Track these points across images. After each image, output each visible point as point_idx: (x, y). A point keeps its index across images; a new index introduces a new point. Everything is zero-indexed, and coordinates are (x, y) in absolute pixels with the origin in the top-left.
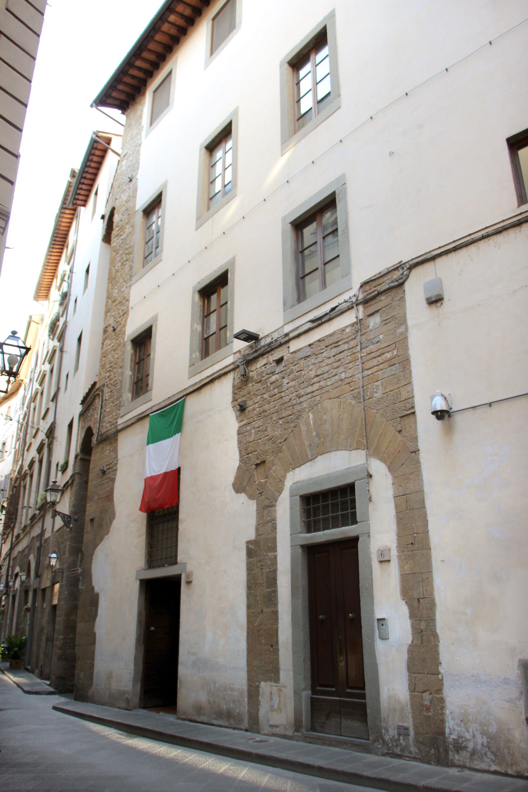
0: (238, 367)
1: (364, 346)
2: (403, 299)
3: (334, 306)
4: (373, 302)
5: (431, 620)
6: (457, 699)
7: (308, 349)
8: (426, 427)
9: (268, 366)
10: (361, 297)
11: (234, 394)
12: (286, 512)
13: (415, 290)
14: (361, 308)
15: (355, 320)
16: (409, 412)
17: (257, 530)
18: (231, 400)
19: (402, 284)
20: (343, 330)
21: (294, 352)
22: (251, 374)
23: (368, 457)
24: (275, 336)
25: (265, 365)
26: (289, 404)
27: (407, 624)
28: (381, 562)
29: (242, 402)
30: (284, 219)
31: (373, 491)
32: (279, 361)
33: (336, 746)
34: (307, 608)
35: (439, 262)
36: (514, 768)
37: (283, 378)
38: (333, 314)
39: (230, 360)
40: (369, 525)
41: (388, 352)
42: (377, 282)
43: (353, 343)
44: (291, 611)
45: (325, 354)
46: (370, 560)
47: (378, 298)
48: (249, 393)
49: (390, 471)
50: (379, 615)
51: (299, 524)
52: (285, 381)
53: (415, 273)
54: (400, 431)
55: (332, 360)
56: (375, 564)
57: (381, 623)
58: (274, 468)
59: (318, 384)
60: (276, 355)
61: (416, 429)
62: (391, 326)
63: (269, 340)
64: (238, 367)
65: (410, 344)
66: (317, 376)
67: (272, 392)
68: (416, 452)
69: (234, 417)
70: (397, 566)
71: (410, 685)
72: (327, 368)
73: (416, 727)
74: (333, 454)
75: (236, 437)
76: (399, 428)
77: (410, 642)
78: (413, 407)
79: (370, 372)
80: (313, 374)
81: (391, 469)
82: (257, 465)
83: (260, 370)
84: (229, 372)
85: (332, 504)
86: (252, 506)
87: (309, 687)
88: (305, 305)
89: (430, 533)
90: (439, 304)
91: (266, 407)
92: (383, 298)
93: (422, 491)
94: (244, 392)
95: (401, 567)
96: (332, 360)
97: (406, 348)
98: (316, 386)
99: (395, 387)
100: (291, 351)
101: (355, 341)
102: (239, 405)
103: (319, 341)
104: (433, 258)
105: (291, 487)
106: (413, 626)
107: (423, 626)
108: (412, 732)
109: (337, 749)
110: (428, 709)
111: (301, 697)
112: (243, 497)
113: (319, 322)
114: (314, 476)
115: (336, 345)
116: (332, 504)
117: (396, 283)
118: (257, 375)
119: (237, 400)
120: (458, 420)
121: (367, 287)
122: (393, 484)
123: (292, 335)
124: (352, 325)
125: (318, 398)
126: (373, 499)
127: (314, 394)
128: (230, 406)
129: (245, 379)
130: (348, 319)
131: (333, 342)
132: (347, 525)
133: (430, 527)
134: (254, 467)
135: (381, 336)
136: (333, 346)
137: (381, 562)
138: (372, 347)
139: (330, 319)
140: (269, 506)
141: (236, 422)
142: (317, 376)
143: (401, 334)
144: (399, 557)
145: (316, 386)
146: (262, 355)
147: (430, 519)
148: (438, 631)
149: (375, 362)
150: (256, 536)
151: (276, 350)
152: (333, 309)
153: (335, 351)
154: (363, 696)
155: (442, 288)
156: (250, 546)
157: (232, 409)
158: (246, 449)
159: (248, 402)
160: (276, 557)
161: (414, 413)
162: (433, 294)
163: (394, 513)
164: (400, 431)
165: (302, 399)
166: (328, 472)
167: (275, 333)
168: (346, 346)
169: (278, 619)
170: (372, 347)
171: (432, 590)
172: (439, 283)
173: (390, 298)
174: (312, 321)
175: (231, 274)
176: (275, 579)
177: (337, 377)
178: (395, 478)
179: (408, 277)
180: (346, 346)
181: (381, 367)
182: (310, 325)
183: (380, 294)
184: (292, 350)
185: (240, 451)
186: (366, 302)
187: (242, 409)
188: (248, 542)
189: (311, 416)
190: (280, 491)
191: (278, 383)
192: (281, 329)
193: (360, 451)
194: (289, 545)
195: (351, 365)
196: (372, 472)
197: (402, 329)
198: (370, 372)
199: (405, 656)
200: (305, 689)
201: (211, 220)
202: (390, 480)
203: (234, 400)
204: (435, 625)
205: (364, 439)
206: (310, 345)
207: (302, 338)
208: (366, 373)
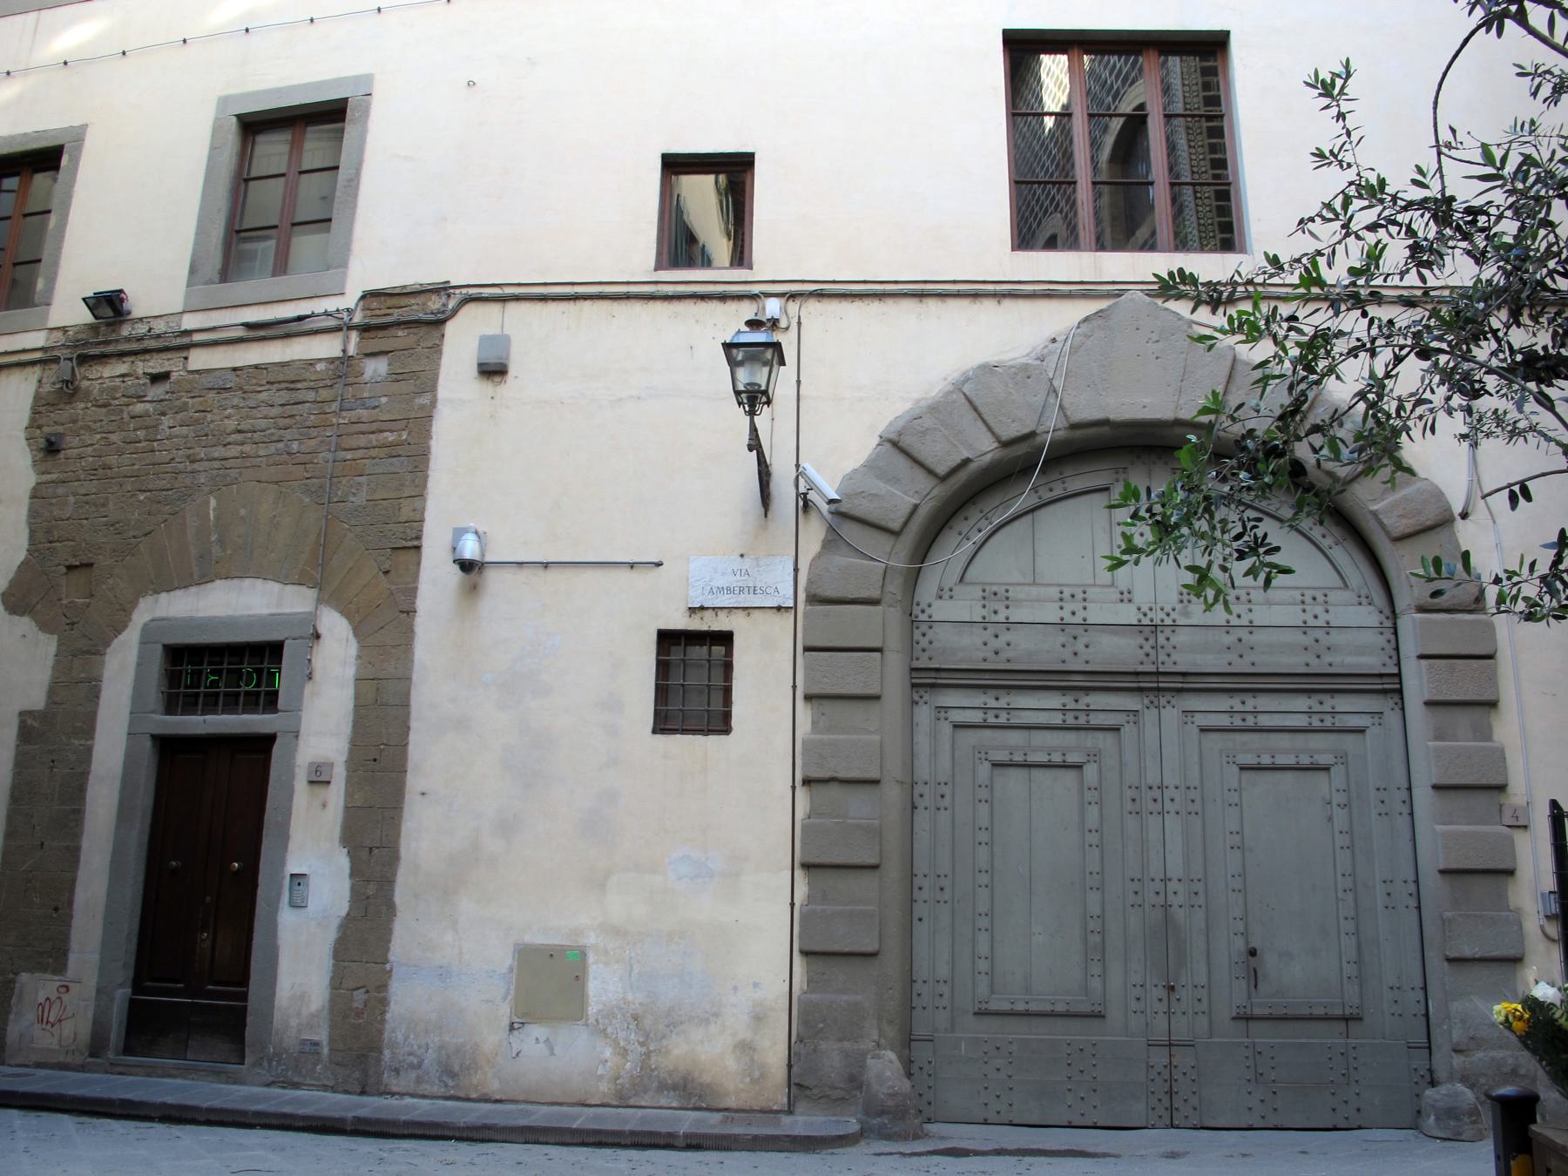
0: (56, 360)
1: (347, 405)
2: (437, 349)
3: (303, 313)
4: (380, 334)
5: (387, 883)
6: (410, 1000)
7: (231, 376)
8: (436, 577)
9: (130, 381)
10: (358, 318)
11: (35, 412)
12: (124, 673)
13: (462, 341)
14: (354, 336)
15: (337, 353)
16: (410, 544)
17: (51, 692)
18: (25, 423)
19: (443, 322)
20: (311, 363)
21: (197, 372)
22: (85, 384)
23: (319, 601)
24: (160, 327)
25: (123, 376)
26: (168, 468)
27: (343, 886)
28: (312, 782)
29: (55, 435)
30: (224, 101)
31: (318, 663)
32: (158, 378)
33: (175, 1077)
34: (145, 847)
35: (512, 307)
36: (1248, 659)
37: (164, 414)
38: (294, 327)
39: (37, 339)
40: (299, 719)
41: (391, 431)
42: (394, 301)
43: (325, 394)
44: (110, 849)
45: (264, 396)
46: (292, 776)
47: (393, 331)
48: (74, 422)
49: (356, 634)
50: (293, 867)
51: (154, 696)
52: (166, 421)
53: (470, 310)
54: (386, 572)
55: (274, 411)
56: (300, 784)
57: (296, 881)
58: (110, 581)
59: (239, 448)
60: (156, 365)
61: (416, 576)
62: (405, 387)
63: (142, 329)
64: (56, 360)
65: (434, 429)
66: (240, 432)
67: (132, 435)
68: (410, 612)
69: (28, 460)
70: (342, 792)
71: (332, 979)
72: (263, 423)
73: (332, 1040)
74: (247, 582)
75: (26, 501)
76: (386, 566)
77: (344, 912)
78: (419, 538)
79: (349, 456)
80: (231, 424)
81: (357, 631)
82: (70, 568)
83: (108, 383)
84: (33, 363)
85: (245, 669)
86: (48, 646)
87: (129, 983)
88: (238, 289)
89: (411, 748)
90: (497, 379)
91: (113, 460)
92: (400, 333)
93: (409, 679)
94: (66, 413)
95: (349, 795)
96: (274, 411)
97: (427, 435)
98: (234, 451)
99: (392, 495)
100: (191, 368)
101: (332, 392)
102: (48, 441)
103: (256, 367)
104: (503, 300)
105: (146, 625)
106: (353, 890)
107: (371, 889)
108: (326, 1051)
109: (179, 1081)
110: (359, 1014)
111: (113, 999)
112: (25, 624)
113: (260, 332)
114: (201, 615)
115: (292, 385)
116: (245, 669)
117: (432, 317)
118: (102, 391)
119: (39, 427)
120: (492, 578)
121: (369, 300)
122: (359, 657)
123: (197, 337)
124: (331, 361)
125: (234, 473)
126: (317, 675)
127: (228, 464)
128: (22, 435)
129: (69, 391)
130: (325, 348)
131: (288, 378)
132: (215, 713)
133: (412, 737)
134: (64, 570)
135: (384, 400)
136: (284, 385)
137: (312, 782)
138: (363, 413)
139: (288, 336)
140: (87, 652)
141: (31, 471)
142: (240, 432)
143: (422, 407)
144: (349, 781)
145: (234, 451)
146: (122, 355)
147: (414, 724)
148: (398, 899)
149: (362, 441)
150: (47, 705)
151: (155, 356)
152: (300, 319)
153: (285, 396)
154: (244, 997)
155: (508, 357)
156: (29, 722)
157: (24, 443)
158: (48, 532)
159: (68, 439)
160: (89, 750)
161: (418, 548)
162: (492, 358)
163: (351, 706)
164: (386, 572)
165: (196, 466)
166: (230, 613)
167: (159, 320)
168: (311, 396)
169: (78, 861)
170: (363, 413)
171: (398, 836)
172: (503, 341)
173: (413, 338)
174: (249, 326)
175: (70, 160)
176: (82, 789)
177: (280, 445)
178: (362, 647)
179: (455, 312)
180: (311, 396)
181: (374, 452)
182: (240, 333)
183: (398, 324)
184: (192, 366)
185: (32, 533)
186: (365, 329)
187: (51, 448)
188: (24, 715)
189: (213, 503)
190: (119, 628)
191: (149, 422)
192: (176, 318)
193: (303, 589)
194: (125, 729)
195: (313, 432)
196: (321, 630)
197: (424, 400)
198: (349, 456)
199: (331, 935)
200: (121, 985)
201: (33, 16)
202: (353, 649)
203: (34, 424)
204: (392, 890)
205: (316, 570)
206: (235, 369)
207: (221, 350)
208: (342, 455)
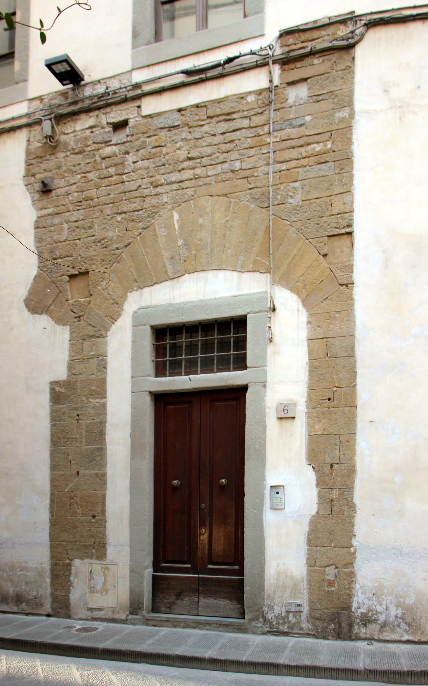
0: (39, 122)
3: (231, 56)
4: (298, 65)
7: (177, 115)
9: (97, 131)
14: (276, 70)
19: (352, 46)
20: (242, 97)
21: (150, 116)
22: (63, 138)
24: (114, 85)
25: (91, 127)
26: (137, 194)
37: (127, 153)
42: (308, 35)
43: (257, 120)
45: (206, 128)
47: (308, 61)
52: (130, 158)
55: (218, 139)
59: (191, 172)
60: (116, 115)
63: (100, 89)
64: (39, 122)
65: (354, 137)
66: (190, 159)
72: (209, 150)
75: (32, 231)
80: (182, 154)
83: (80, 135)
92: (316, 61)
98: (188, 174)
103: (197, 106)
115: (228, 117)
118: (77, 142)
123: (147, 88)
124: (259, 92)
125: (190, 192)
129: (52, 144)
131: (224, 112)
136: (221, 118)
142: (190, 159)
145: (188, 174)
146: (88, 110)
151: (114, 107)
152: (230, 60)
153: (224, 126)
167: (113, 80)
168: (245, 123)
177: (225, 166)
180: (245, 123)
183: (313, 53)
189: (176, 216)
191: (117, 160)
192: (127, 76)
195: (252, 152)
206: (180, 110)
